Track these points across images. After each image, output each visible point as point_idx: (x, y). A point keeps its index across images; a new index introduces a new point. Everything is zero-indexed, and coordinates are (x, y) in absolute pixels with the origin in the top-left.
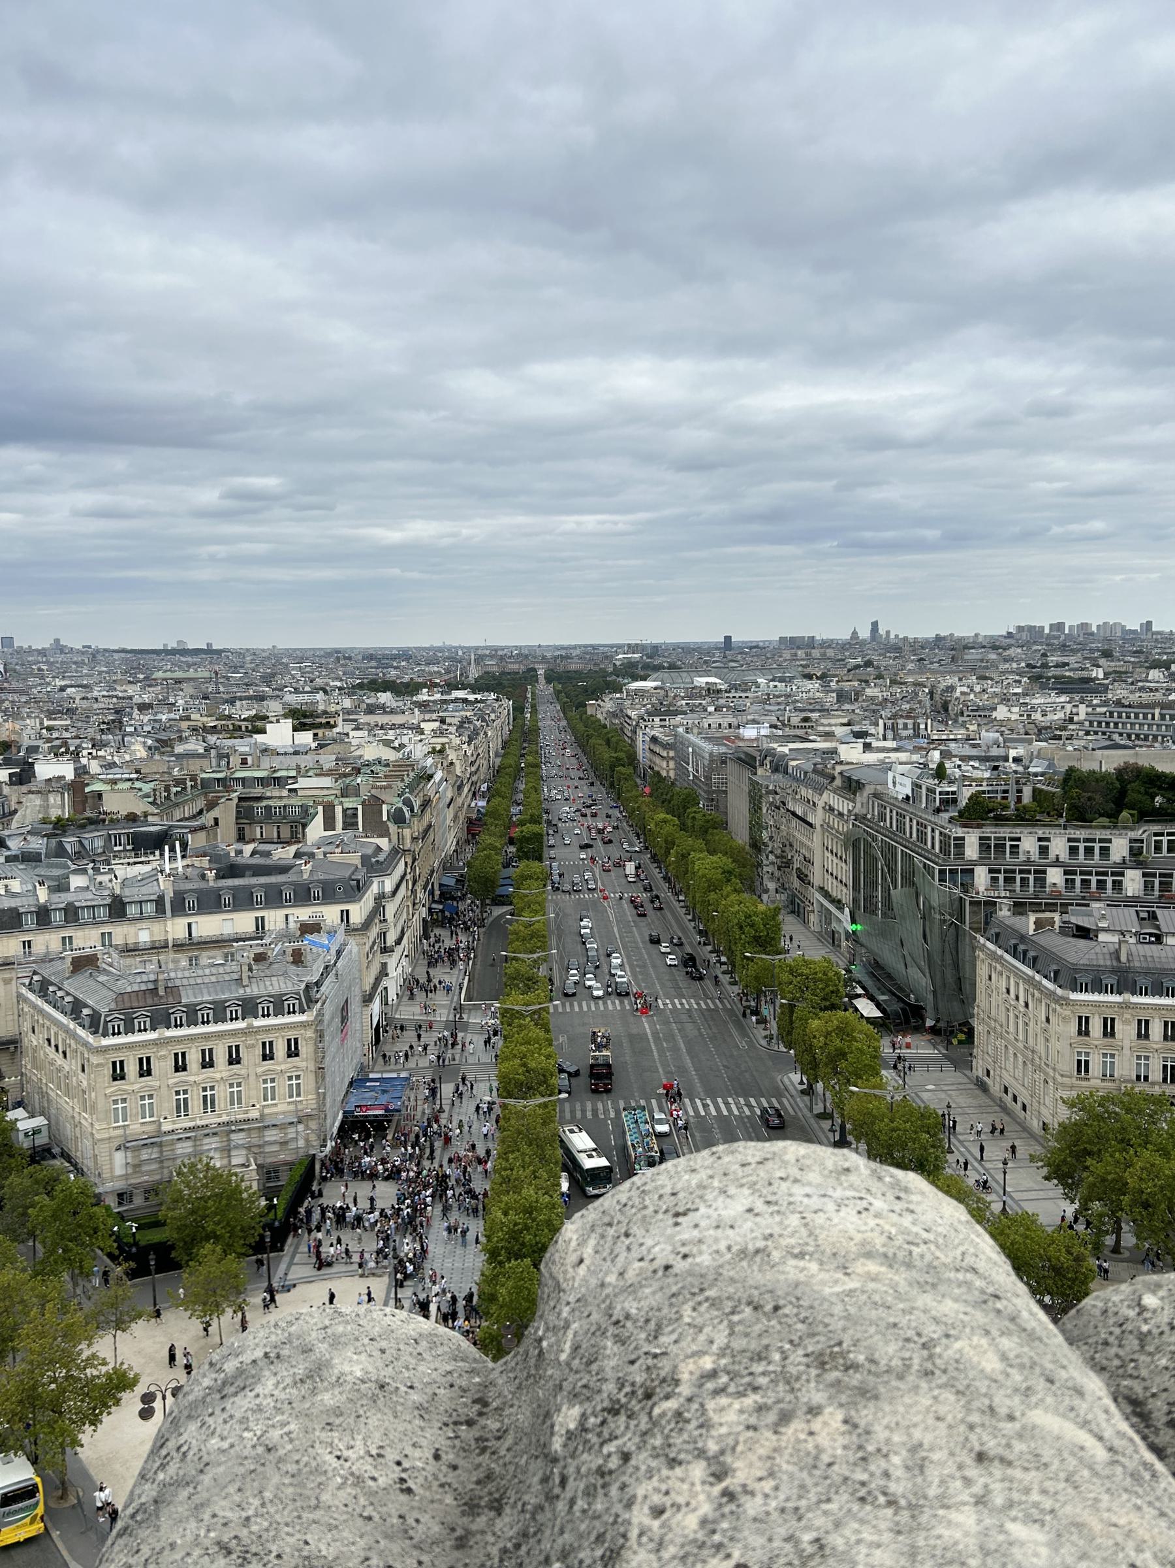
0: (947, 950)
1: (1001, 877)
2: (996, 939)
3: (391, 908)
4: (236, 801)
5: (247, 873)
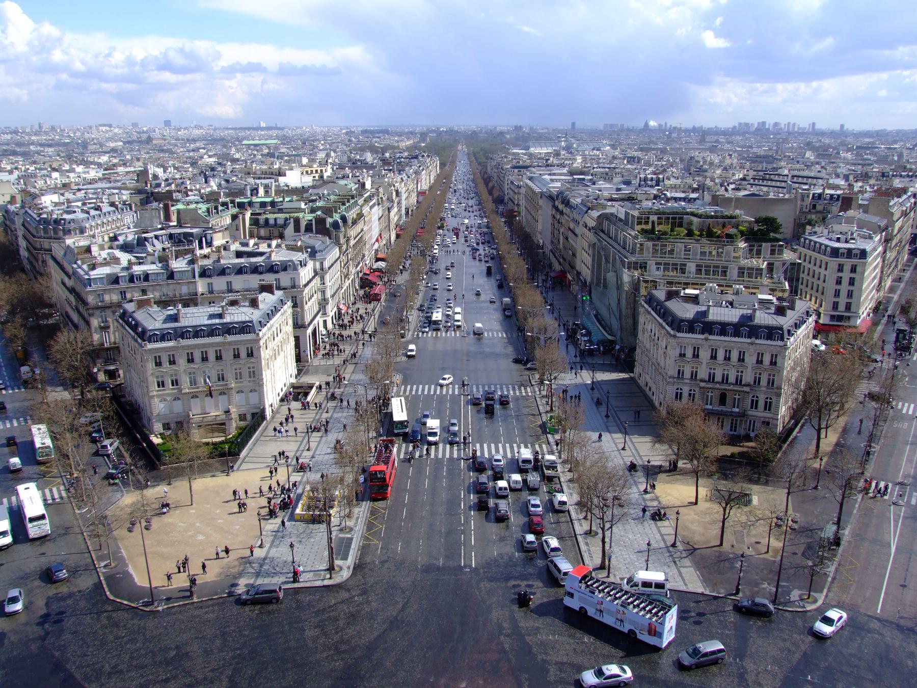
1: (662, 267)
3: (327, 277)
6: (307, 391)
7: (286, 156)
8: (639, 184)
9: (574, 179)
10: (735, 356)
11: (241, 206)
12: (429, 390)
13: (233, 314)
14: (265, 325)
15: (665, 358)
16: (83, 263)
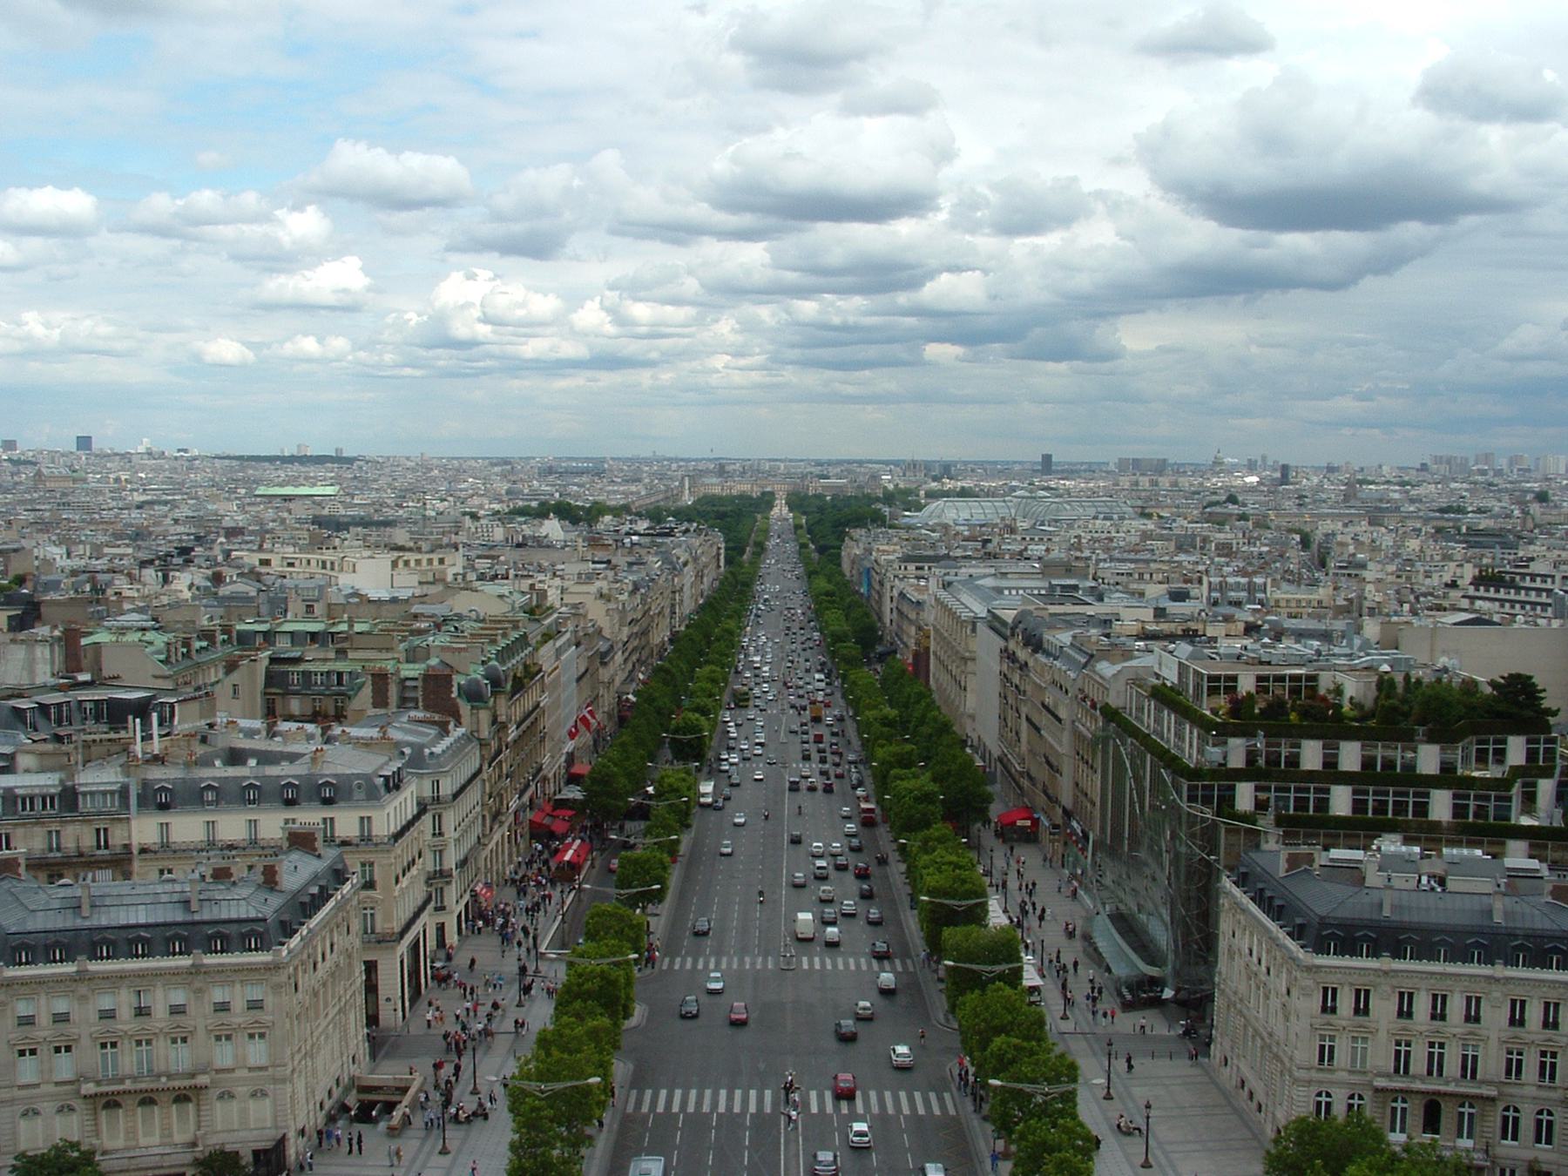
2: (1242, 881)
3: (450, 819)
4: (266, 662)
5: (252, 762)
7: (357, 525)
8: (1209, 598)
9: (1052, 587)
10: (1456, 1007)
11: (245, 639)
14: (296, 931)
15: (1287, 1019)
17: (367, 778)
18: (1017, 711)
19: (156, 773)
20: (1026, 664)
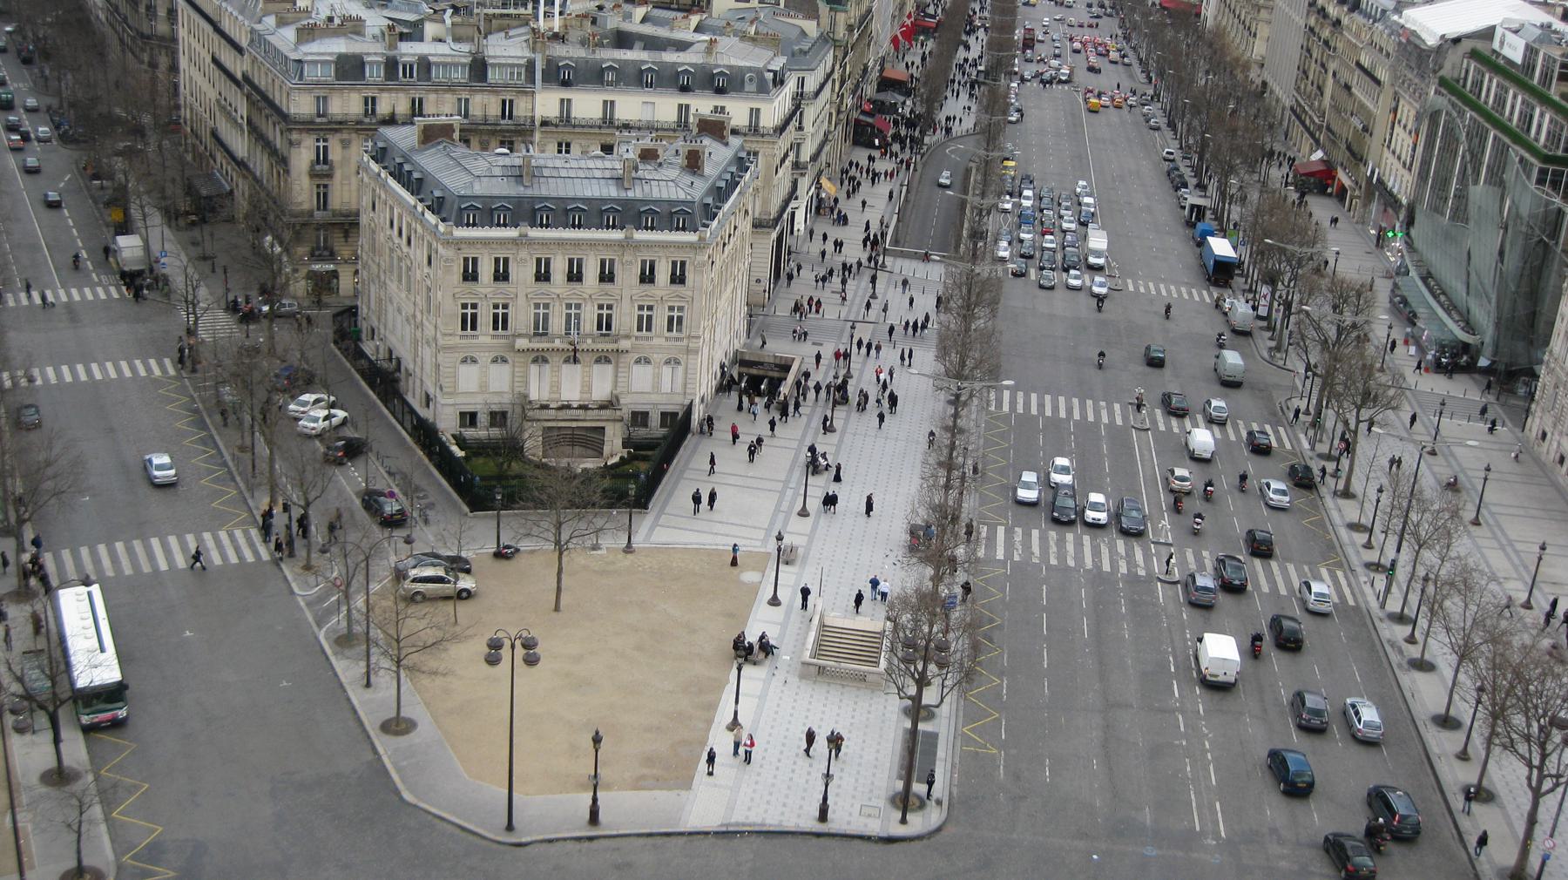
0: (1527, 272)
3: (810, 112)
5: (638, 44)
6: (776, 375)
12: (1055, 408)
13: (648, 181)
14: (715, 215)
16: (282, 23)
17: (759, 73)
18: (1323, 65)
19: (559, 50)
20: (1337, 23)
